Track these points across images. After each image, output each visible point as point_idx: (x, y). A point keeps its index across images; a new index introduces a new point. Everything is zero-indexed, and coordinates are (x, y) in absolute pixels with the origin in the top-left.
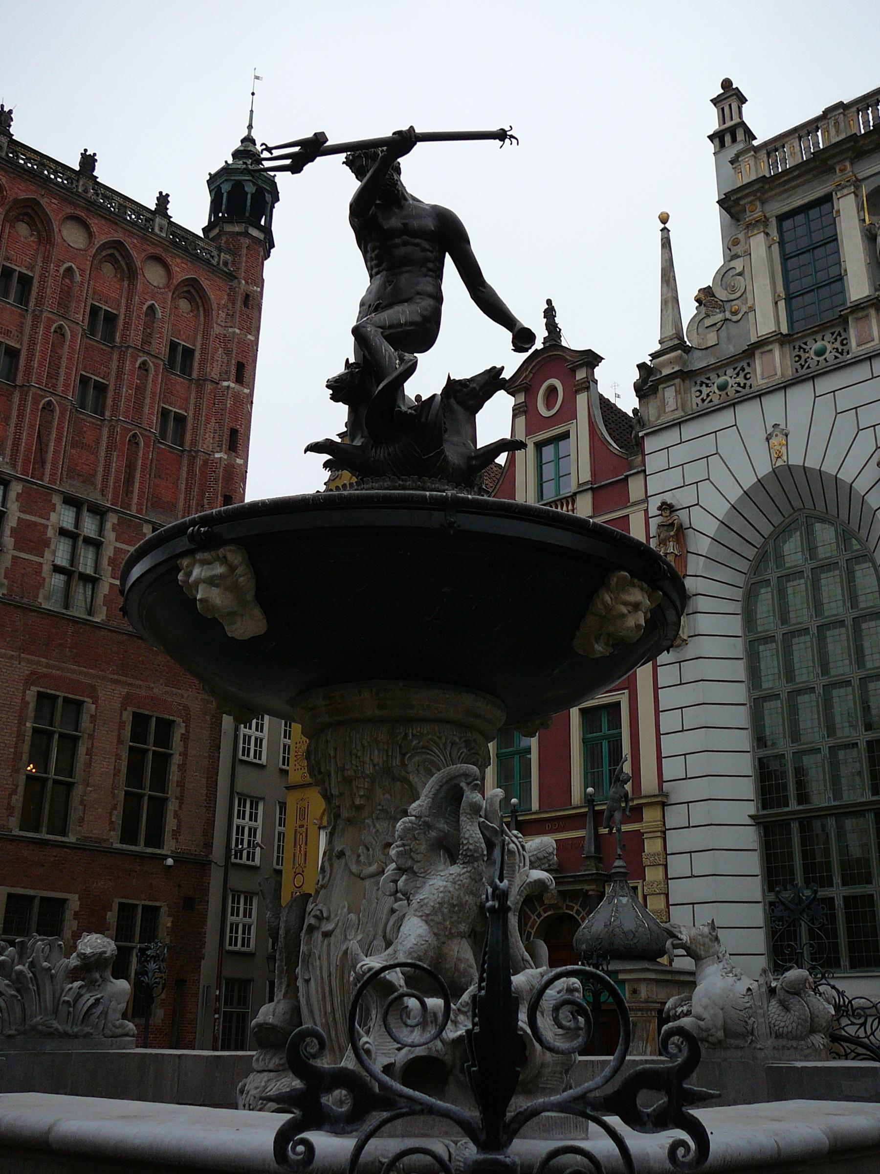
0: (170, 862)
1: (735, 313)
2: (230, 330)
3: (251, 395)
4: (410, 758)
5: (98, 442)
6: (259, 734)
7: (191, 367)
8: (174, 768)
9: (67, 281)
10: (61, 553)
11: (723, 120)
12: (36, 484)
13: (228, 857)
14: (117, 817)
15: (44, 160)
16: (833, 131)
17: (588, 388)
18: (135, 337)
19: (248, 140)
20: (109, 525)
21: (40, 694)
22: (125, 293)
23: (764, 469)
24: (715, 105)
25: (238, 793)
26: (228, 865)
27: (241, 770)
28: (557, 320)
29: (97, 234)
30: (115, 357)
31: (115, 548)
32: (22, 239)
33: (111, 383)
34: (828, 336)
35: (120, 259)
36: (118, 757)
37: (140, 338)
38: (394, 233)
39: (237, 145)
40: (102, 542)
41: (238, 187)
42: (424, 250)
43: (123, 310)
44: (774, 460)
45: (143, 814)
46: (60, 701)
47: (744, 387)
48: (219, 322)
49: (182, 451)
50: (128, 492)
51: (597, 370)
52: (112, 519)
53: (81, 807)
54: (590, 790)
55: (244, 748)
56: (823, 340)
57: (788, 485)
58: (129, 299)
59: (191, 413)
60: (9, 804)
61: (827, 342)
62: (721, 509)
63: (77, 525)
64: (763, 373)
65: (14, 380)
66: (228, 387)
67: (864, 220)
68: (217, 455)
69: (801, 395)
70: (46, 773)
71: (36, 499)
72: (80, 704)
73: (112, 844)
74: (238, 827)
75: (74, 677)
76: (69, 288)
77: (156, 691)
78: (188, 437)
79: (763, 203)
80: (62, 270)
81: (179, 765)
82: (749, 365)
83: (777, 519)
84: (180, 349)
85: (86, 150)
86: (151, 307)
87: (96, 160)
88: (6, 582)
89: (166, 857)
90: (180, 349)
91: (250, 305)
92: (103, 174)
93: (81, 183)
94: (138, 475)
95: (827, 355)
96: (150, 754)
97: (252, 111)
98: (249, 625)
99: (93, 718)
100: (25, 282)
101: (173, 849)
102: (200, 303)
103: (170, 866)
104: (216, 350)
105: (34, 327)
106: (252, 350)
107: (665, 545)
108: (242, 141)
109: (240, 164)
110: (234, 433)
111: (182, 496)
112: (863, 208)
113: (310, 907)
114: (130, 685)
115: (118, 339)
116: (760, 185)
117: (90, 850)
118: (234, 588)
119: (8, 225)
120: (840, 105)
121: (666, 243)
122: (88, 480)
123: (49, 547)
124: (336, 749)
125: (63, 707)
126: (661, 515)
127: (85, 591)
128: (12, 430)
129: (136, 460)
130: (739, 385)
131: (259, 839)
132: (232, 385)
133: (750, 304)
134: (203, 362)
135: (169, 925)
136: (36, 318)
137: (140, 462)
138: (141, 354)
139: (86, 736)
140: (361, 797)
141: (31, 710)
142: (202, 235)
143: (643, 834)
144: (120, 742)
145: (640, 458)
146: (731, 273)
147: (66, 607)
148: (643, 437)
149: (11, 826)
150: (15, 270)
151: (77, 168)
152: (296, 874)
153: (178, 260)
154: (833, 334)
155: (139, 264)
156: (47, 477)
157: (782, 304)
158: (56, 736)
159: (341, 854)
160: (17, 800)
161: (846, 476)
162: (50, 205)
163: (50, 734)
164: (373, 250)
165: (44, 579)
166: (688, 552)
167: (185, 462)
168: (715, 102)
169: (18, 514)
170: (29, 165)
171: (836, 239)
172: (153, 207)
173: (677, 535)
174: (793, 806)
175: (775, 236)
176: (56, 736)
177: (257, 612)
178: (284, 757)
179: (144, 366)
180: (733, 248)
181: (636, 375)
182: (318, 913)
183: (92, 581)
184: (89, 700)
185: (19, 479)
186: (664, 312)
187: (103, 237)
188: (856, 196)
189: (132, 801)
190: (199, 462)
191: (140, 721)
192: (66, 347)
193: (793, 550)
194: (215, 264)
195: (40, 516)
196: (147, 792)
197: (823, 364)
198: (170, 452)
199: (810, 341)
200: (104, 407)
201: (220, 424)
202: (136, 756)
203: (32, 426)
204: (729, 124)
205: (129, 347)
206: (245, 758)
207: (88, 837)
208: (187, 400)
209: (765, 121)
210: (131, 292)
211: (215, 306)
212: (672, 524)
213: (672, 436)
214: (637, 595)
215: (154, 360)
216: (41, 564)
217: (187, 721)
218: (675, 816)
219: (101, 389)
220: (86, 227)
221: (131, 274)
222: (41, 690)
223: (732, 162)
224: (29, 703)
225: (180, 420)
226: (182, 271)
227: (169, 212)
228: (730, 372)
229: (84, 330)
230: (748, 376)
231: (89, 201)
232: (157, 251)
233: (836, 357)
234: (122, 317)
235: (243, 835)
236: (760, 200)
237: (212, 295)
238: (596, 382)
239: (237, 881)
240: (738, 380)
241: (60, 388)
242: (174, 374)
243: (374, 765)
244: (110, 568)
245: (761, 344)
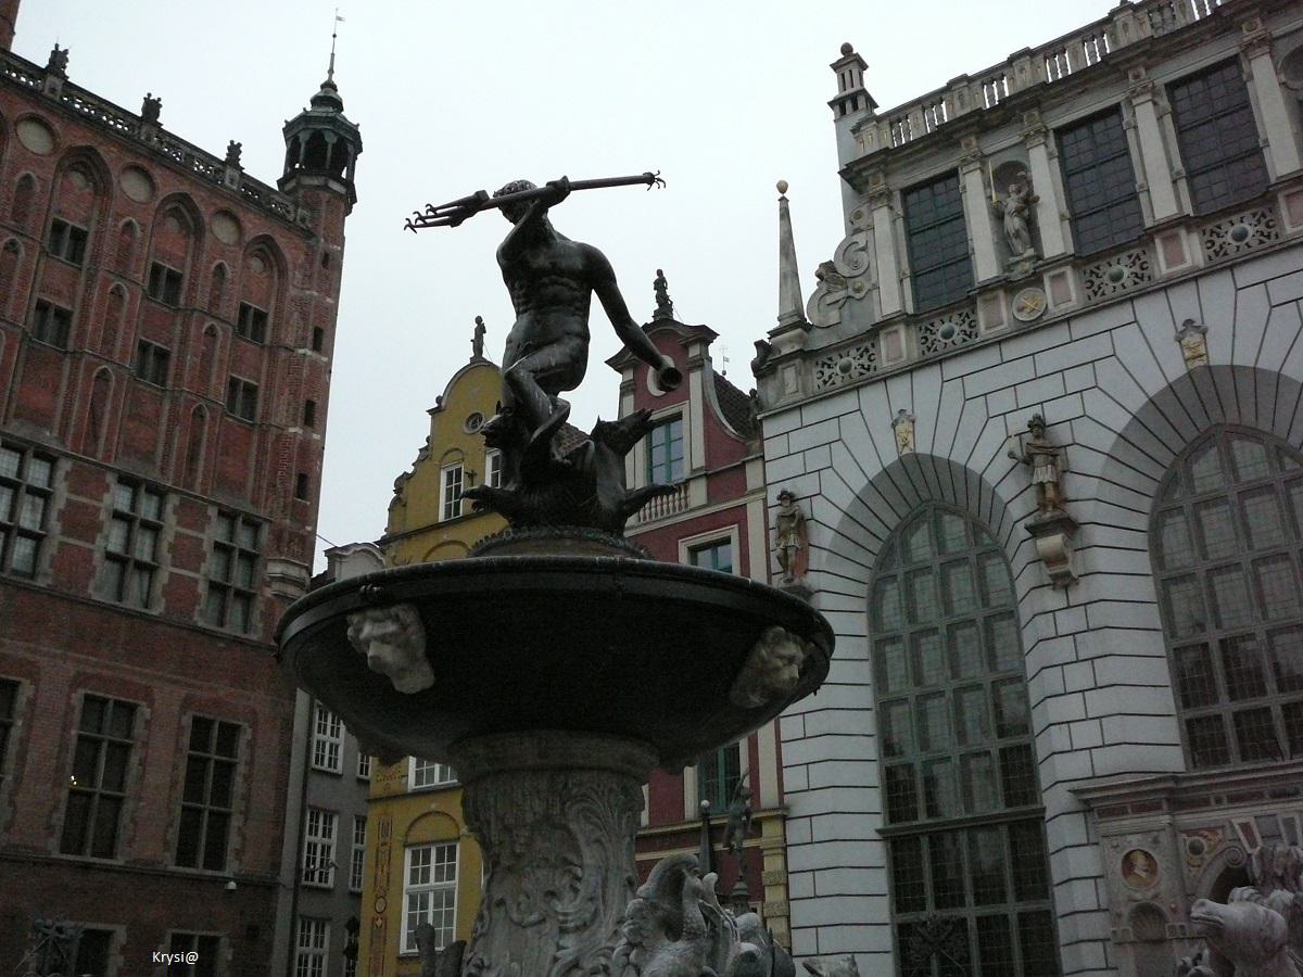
0: (232, 885)
1: (858, 290)
2: (308, 292)
3: (329, 364)
4: (570, 808)
5: (158, 414)
6: (333, 740)
7: (263, 333)
8: (239, 779)
9: (127, 237)
10: (114, 538)
11: (843, 85)
12: (87, 461)
13: (297, 882)
14: (173, 835)
15: (103, 105)
16: (957, 104)
17: (701, 367)
18: (202, 299)
19: (329, 86)
20: (169, 508)
21: (88, 698)
22: (191, 250)
23: (890, 458)
24: (835, 70)
25: (310, 806)
26: (297, 888)
27: (314, 780)
28: (668, 292)
29: (160, 186)
30: (179, 320)
31: (176, 532)
32: (77, 191)
33: (174, 350)
34: (956, 318)
35: (186, 213)
36: (175, 767)
37: (206, 299)
38: (543, 272)
39: (317, 90)
40: (162, 527)
41: (317, 139)
42: (571, 288)
43: (187, 271)
44: (900, 447)
45: (202, 832)
46: (111, 705)
47: (868, 370)
48: (295, 283)
49: (253, 425)
50: (191, 471)
51: (711, 347)
52: (173, 501)
54: (705, 803)
55: (317, 756)
56: (950, 321)
57: (916, 476)
58: (196, 258)
59: (263, 382)
61: (954, 324)
62: (845, 500)
63: (133, 507)
64: (888, 356)
65: (65, 346)
66: (304, 355)
67: (991, 197)
68: (292, 430)
69: (928, 379)
71: (88, 478)
72: (131, 709)
73: (166, 866)
74: (309, 844)
76: (129, 245)
77: (221, 693)
78: (259, 410)
79: (886, 175)
80: (121, 224)
81: (244, 775)
82: (873, 345)
83: (903, 511)
84: (252, 311)
85: (149, 95)
86: (220, 267)
87: (161, 106)
88: (51, 571)
89: (226, 880)
90: (252, 311)
91: (330, 265)
92: (168, 121)
93: (144, 130)
94: (203, 452)
95: (954, 337)
96: (212, 764)
97: (333, 55)
98: (417, 680)
99: (147, 722)
100: (79, 237)
101: (236, 870)
102: (274, 263)
103: (232, 891)
104: (292, 314)
105: (89, 287)
106: (332, 312)
107: (785, 537)
108: (322, 87)
109: (322, 111)
110: (310, 405)
111: (251, 477)
112: (989, 186)
113: (467, 956)
114: (190, 685)
115: (182, 301)
116: (883, 156)
118: (405, 646)
119: (61, 174)
120: (964, 78)
121: (785, 214)
122: (148, 457)
123: (101, 532)
124: (496, 797)
126: (780, 505)
127: (141, 581)
128: (61, 401)
129: (202, 434)
130: (863, 366)
131: (333, 857)
132: (309, 353)
133: (874, 280)
134: (276, 327)
135: (230, 958)
136: (91, 278)
137: (205, 439)
138: (207, 318)
139: (139, 744)
140: (521, 845)
141: (77, 716)
142: (277, 189)
143: (762, 851)
144: (178, 750)
145: (757, 443)
146: (854, 248)
147: (120, 599)
148: (761, 421)
150: (67, 224)
151: (139, 114)
152: (378, 898)
153: (251, 216)
154: (960, 315)
155: (207, 219)
156: (100, 455)
157: (907, 283)
158: (105, 745)
159: (501, 903)
160: (59, 818)
161: (976, 466)
162: (109, 154)
163: (97, 743)
164: (521, 287)
165: (95, 567)
166: (811, 545)
167: (255, 438)
168: (836, 67)
169: (66, 495)
170: (86, 110)
171: (963, 216)
172: (223, 156)
173: (798, 526)
174: (923, 819)
175: (899, 210)
176: (105, 745)
177: (426, 668)
178: (362, 765)
179: (211, 332)
180: (856, 222)
181: (753, 354)
182: (479, 962)
183: (149, 569)
185: (67, 456)
186: (783, 286)
187: (167, 189)
188: (982, 171)
189: (191, 818)
190: (271, 438)
191: (201, 726)
192: (125, 310)
193: (920, 544)
194: (292, 220)
195: (92, 497)
196: (207, 806)
197: (951, 347)
198: (239, 426)
199: (937, 322)
200: (165, 376)
201: (295, 394)
202: (196, 767)
203: (84, 397)
204: (850, 91)
205: (195, 310)
206: (319, 767)
208: (258, 370)
209: (889, 89)
210: (198, 249)
211: (290, 266)
212: (793, 516)
213: (792, 421)
214: (791, 648)
215: (221, 324)
216: (92, 551)
217: (254, 725)
218: (797, 830)
219: (163, 356)
220: (148, 177)
221: (197, 230)
222: (90, 692)
223: (854, 131)
224: (74, 708)
225: (250, 391)
226: (255, 226)
227: (241, 163)
228: (853, 352)
229: (144, 290)
230: (872, 358)
231: (153, 150)
232: (225, 205)
233: (964, 340)
234: (187, 276)
235: (315, 853)
236: (883, 172)
237: (288, 256)
238: (710, 360)
239: (310, 906)
240: (861, 361)
241: (116, 356)
242: (245, 340)
243: (535, 814)
244: (170, 556)
245: (886, 324)
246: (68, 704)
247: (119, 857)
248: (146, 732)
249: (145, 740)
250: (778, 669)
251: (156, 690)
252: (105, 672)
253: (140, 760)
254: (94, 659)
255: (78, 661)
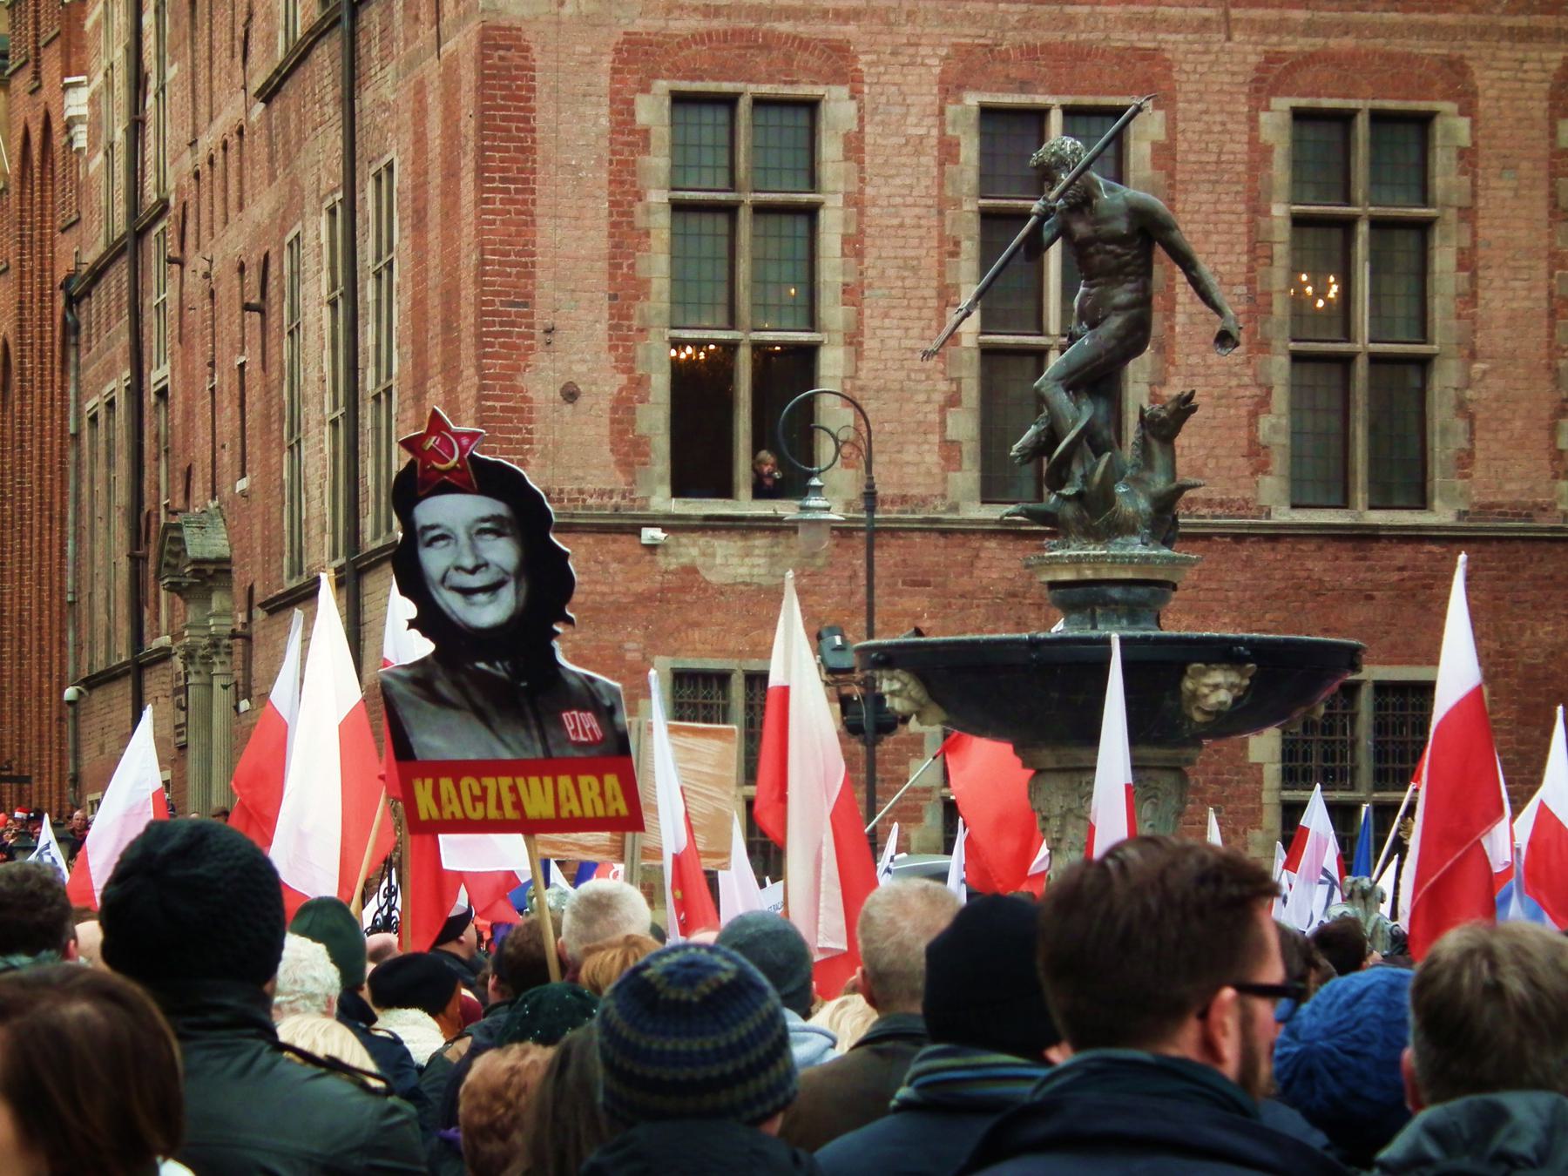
21: (1299, 115)
46: (1362, 126)
53: (1461, 424)
60: (1252, 440)
70: (1348, 341)
72: (1424, 121)
75: (1396, 46)
99: (1467, 158)
117: (1500, 539)
118: (910, 698)
125: (1375, 143)
139: (1451, 214)
141: (1280, 170)
149: (1265, 498)
158: (1363, 229)
160: (1275, 426)
176: (1363, 229)
184: (1446, 107)
207: (1491, 506)
214: (1217, 677)
222: (1303, 102)
246: (1253, 142)
247: (1437, 503)
248: (1466, 180)
249: (1466, 202)
250: (1206, 696)
251: (1474, 65)
252: (1333, 43)
253: (1461, 251)
254: (1299, 15)
255: (1265, 28)
